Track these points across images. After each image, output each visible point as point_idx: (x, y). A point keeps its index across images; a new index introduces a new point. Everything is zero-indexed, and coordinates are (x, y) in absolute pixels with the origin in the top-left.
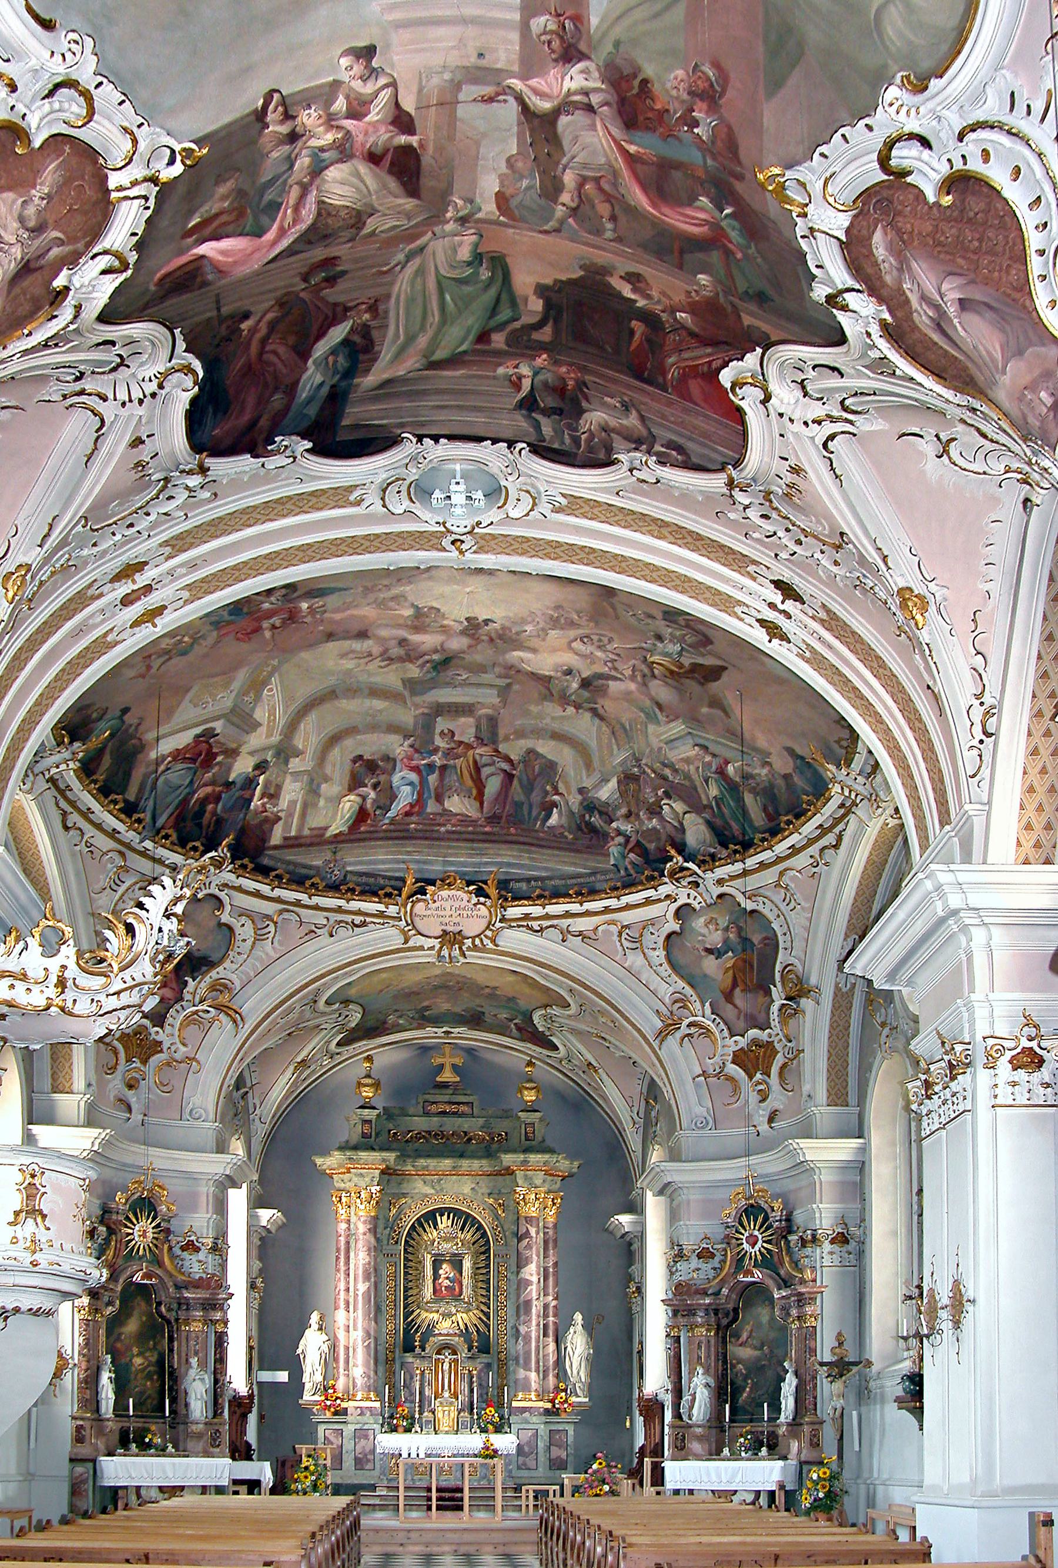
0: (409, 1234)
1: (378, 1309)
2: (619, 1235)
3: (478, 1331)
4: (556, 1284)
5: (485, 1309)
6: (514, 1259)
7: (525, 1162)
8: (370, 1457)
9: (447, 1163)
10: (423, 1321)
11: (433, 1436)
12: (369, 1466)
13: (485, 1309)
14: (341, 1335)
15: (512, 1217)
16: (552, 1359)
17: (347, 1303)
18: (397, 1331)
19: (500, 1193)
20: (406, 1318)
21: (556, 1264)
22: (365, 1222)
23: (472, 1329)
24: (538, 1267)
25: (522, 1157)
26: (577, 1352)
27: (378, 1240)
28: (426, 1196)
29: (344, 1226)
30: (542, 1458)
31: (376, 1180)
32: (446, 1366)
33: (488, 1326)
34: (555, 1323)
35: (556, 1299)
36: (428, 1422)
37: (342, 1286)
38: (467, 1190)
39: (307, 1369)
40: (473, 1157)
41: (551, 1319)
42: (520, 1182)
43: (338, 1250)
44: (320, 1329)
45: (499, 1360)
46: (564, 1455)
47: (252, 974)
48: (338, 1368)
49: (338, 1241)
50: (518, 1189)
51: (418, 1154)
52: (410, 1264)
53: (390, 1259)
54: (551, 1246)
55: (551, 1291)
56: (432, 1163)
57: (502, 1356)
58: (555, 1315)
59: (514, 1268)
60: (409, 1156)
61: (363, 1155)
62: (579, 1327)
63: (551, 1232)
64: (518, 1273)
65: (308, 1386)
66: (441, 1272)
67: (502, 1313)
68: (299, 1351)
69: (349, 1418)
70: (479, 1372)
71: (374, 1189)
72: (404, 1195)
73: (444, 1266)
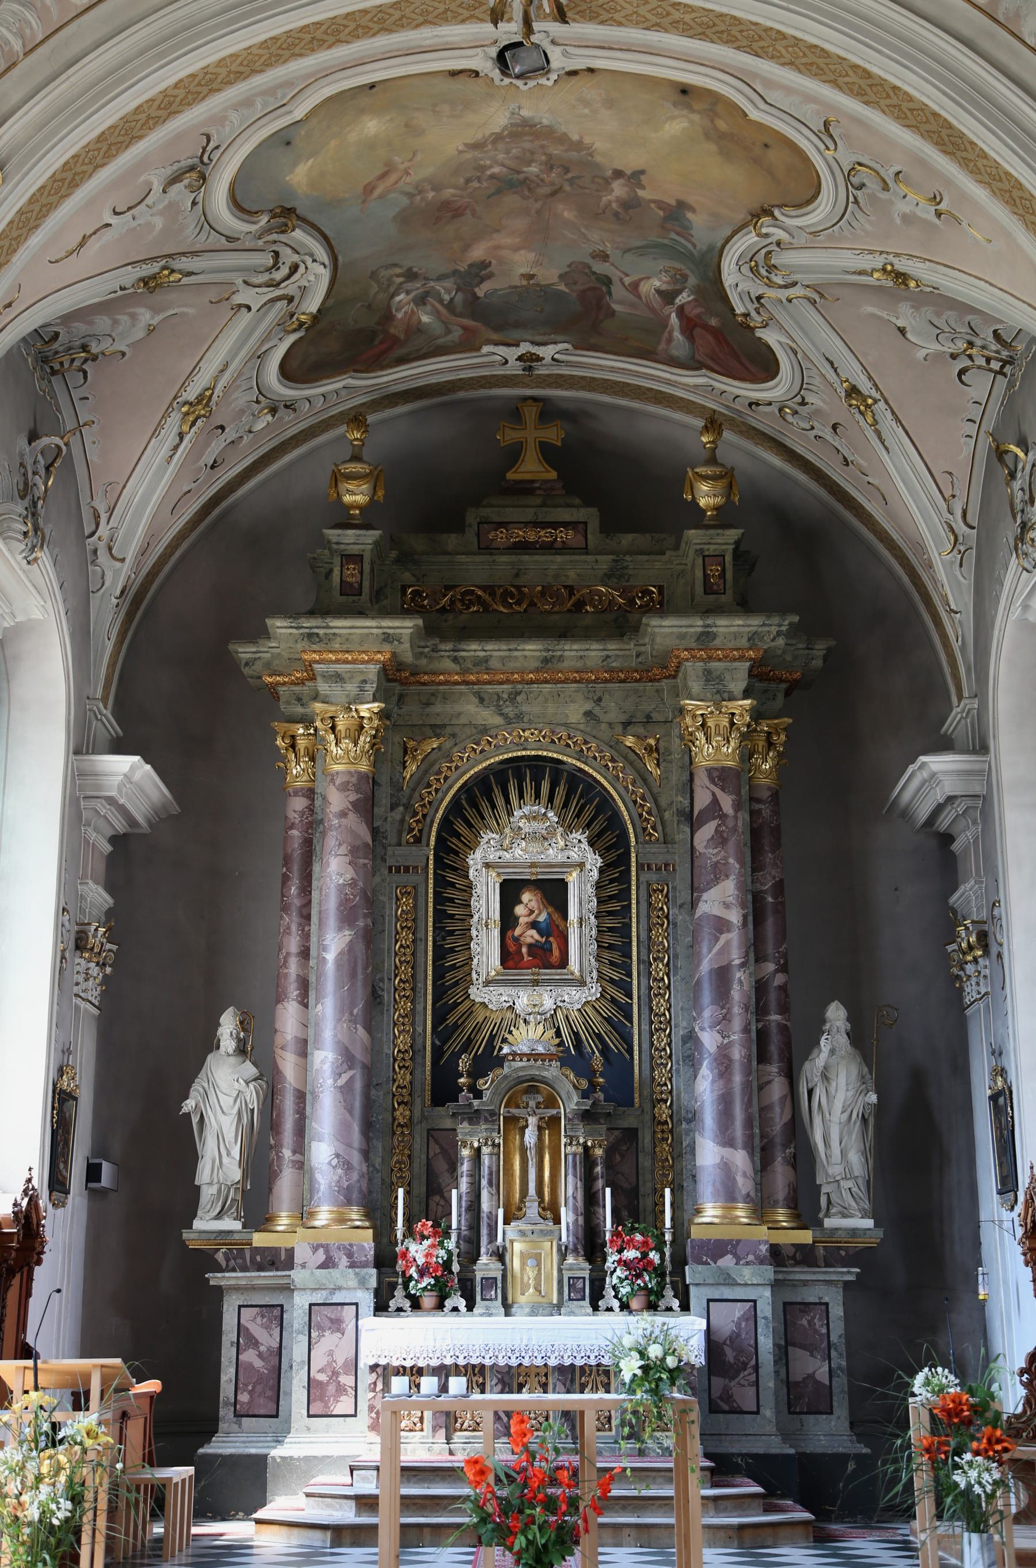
0: (446, 823)
1: (374, 998)
2: (923, 812)
3: (605, 1051)
4: (782, 935)
5: (622, 999)
6: (683, 871)
7: (706, 637)
8: (347, 1380)
9: (531, 650)
10: (478, 1028)
11: (500, 1319)
12: (344, 1405)
13: (622, 999)
14: (288, 1065)
15: (677, 777)
16: (779, 1118)
17: (304, 985)
18: (415, 1050)
19: (648, 720)
20: (439, 1019)
21: (779, 888)
22: (344, 788)
23: (590, 1045)
24: (741, 887)
25: (696, 624)
26: (838, 1105)
27: (375, 832)
28: (484, 730)
29: (298, 804)
30: (768, 1383)
31: (371, 688)
32: (530, 1137)
33: (627, 1039)
34: (784, 1029)
35: (783, 969)
36: (489, 1282)
37: (293, 944)
38: (575, 712)
39: (209, 1149)
40: (588, 634)
41: (775, 1017)
42: (696, 687)
43: (287, 860)
44: (242, 1051)
45: (656, 1121)
46: (822, 1373)
47: (17, 46)
48: (278, 1146)
49: (286, 839)
50: (689, 703)
51: (466, 633)
52: (450, 893)
53: (403, 878)
54: (766, 842)
55: (770, 948)
56: (494, 650)
57: (663, 1112)
58: (784, 1009)
59: (684, 896)
60: (444, 638)
61: (340, 625)
62: (843, 1040)
63: (766, 811)
64: (693, 904)
65: (208, 1193)
66: (519, 910)
67: (659, 1005)
68: (189, 1105)
69: (297, 1275)
70: (610, 1152)
71: (367, 709)
72: (437, 730)
73: (526, 897)
